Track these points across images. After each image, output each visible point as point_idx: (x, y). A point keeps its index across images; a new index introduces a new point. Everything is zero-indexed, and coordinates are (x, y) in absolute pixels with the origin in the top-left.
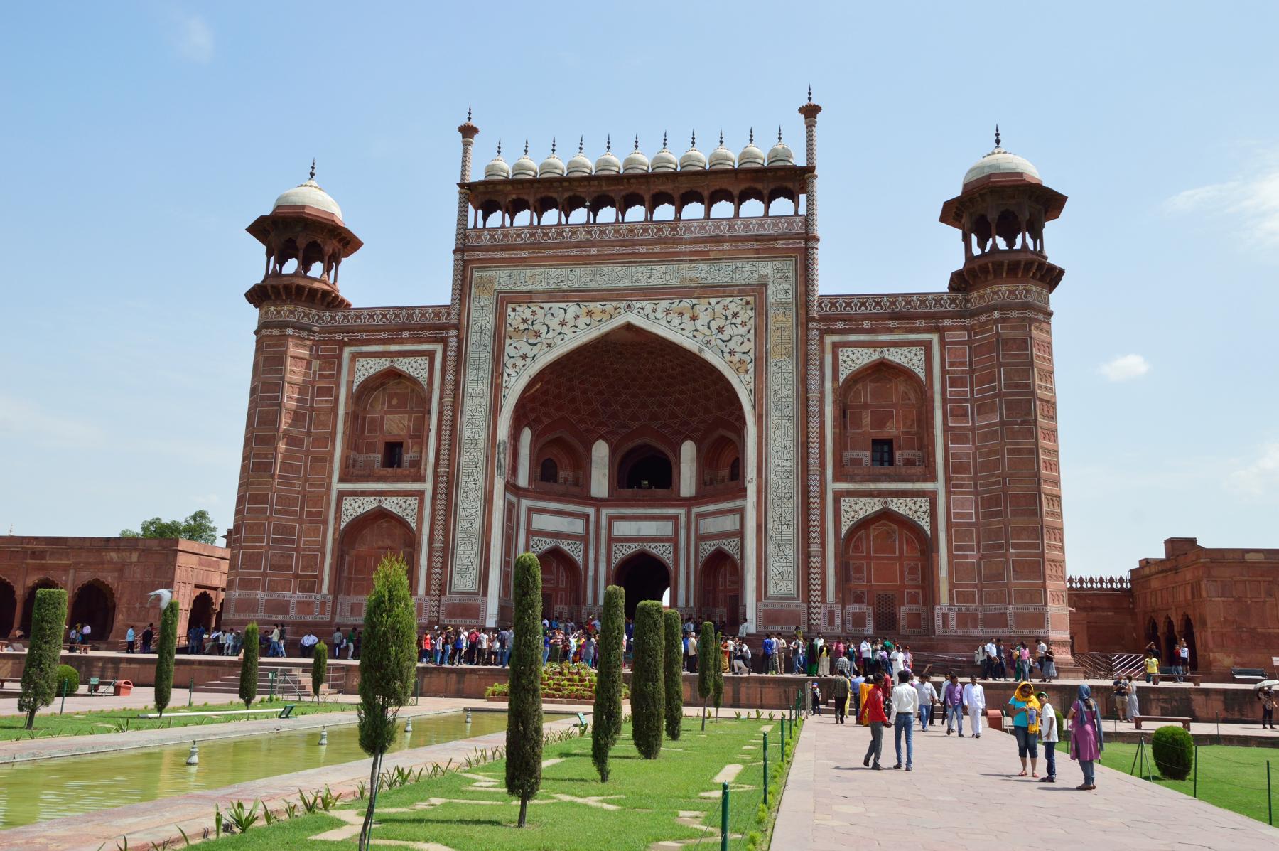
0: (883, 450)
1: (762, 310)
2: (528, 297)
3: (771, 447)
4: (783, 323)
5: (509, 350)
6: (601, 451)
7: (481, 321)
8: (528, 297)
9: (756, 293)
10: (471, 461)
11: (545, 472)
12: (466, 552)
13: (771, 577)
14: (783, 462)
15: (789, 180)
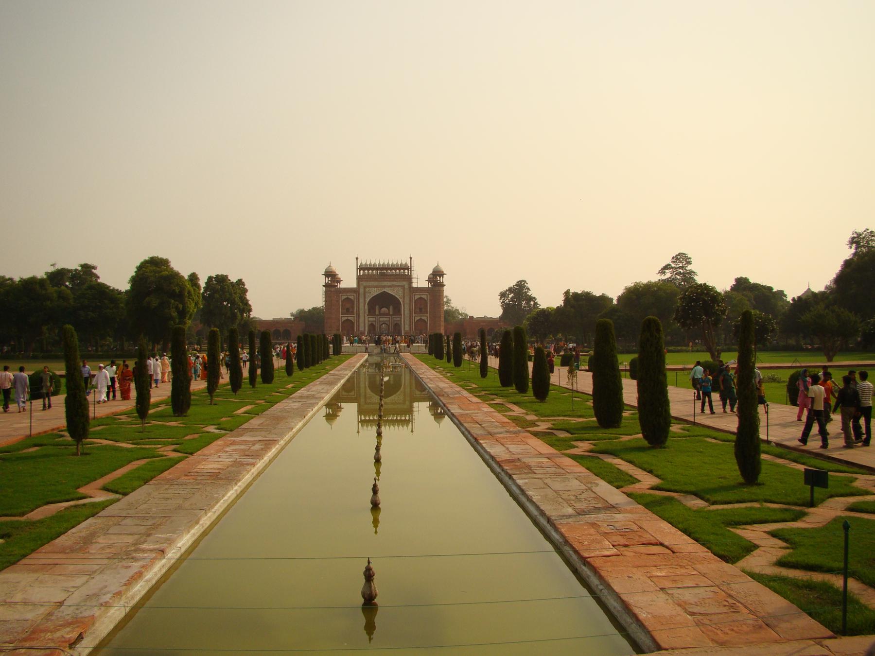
0: (421, 309)
1: (404, 289)
2: (369, 287)
3: (405, 309)
4: (407, 291)
5: (367, 295)
6: (377, 307)
7: (362, 290)
8: (369, 287)
9: (403, 287)
10: (362, 312)
11: (369, 310)
12: (362, 325)
13: (405, 327)
14: (407, 312)
15: (408, 269)
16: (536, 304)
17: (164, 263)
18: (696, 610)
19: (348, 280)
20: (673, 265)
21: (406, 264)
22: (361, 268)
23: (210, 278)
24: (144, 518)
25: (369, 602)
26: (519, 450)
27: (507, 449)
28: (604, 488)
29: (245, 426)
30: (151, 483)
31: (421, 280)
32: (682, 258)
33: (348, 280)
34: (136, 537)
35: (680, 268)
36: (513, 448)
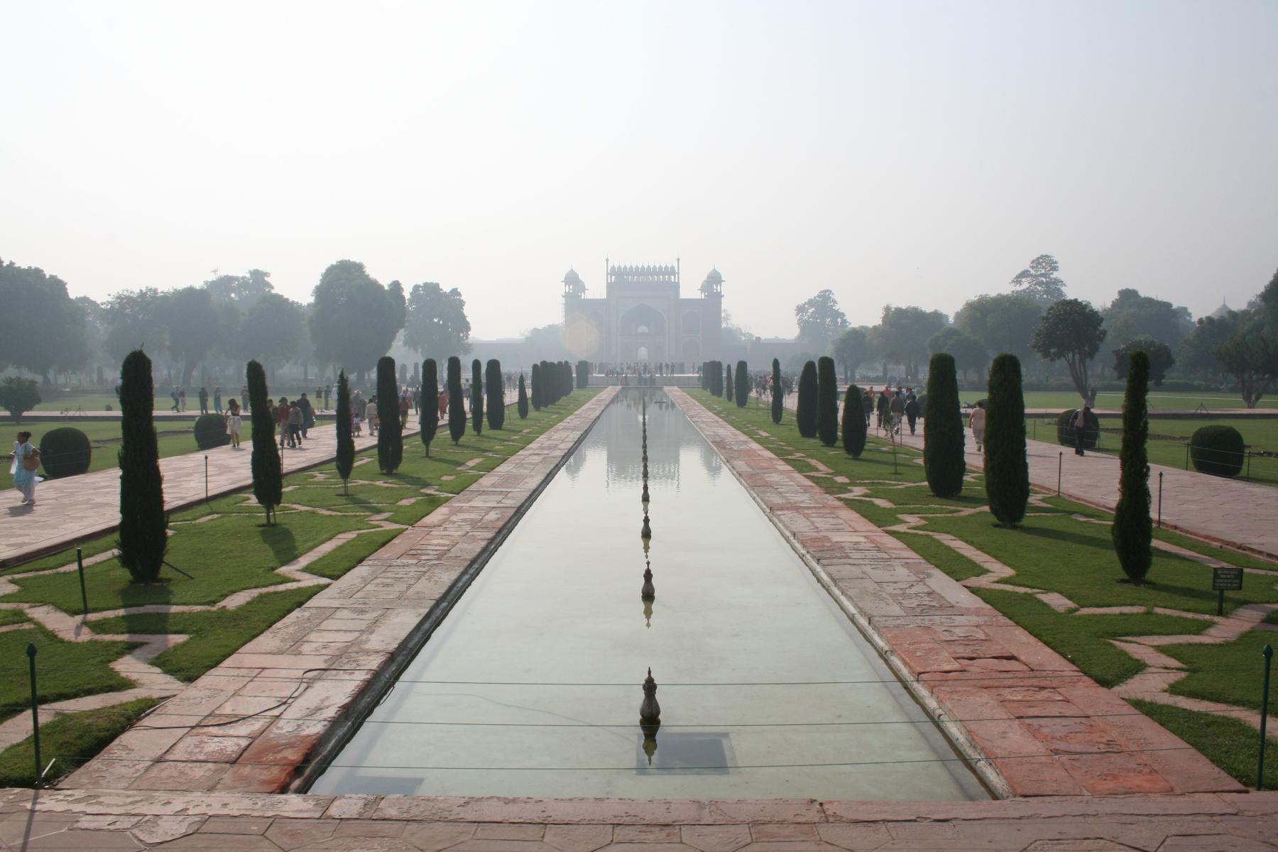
16: (844, 321)
17: (359, 267)
18: (1062, 746)
19: (596, 289)
20: (1032, 272)
21: (673, 267)
22: (614, 272)
23: (416, 287)
24: (363, 612)
25: (650, 721)
26: (828, 526)
27: (813, 523)
28: (941, 582)
29: (474, 487)
30: (364, 563)
31: (690, 289)
32: (1046, 263)
33: (596, 289)
34: (357, 634)
35: (1042, 275)
36: (820, 522)
